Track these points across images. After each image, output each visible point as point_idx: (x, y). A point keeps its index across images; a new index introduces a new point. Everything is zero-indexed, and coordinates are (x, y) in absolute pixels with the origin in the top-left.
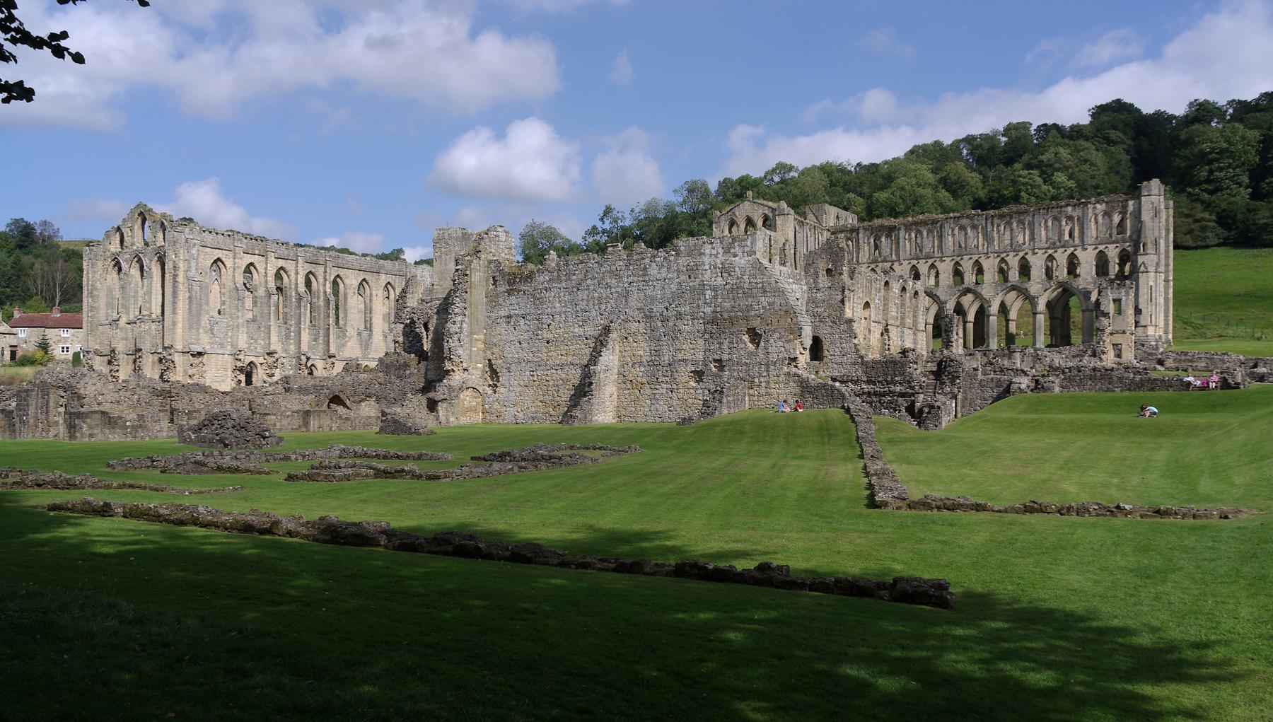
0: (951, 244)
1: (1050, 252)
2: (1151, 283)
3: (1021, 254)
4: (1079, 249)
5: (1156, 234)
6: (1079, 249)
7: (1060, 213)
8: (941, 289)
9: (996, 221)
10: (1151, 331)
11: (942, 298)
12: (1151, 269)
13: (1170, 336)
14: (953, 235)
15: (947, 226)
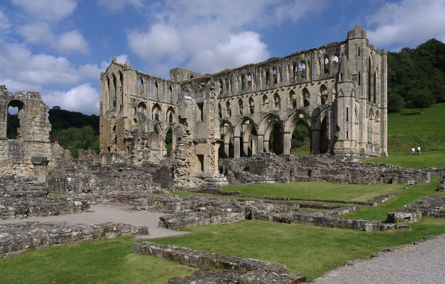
0: (237, 87)
1: (292, 88)
2: (347, 106)
3: (275, 91)
4: (309, 84)
5: (360, 68)
6: (309, 84)
7: (297, 59)
8: (232, 118)
9: (261, 69)
10: (347, 145)
11: (233, 124)
12: (347, 94)
13: (386, 150)
14: (239, 81)
15: (234, 75)
